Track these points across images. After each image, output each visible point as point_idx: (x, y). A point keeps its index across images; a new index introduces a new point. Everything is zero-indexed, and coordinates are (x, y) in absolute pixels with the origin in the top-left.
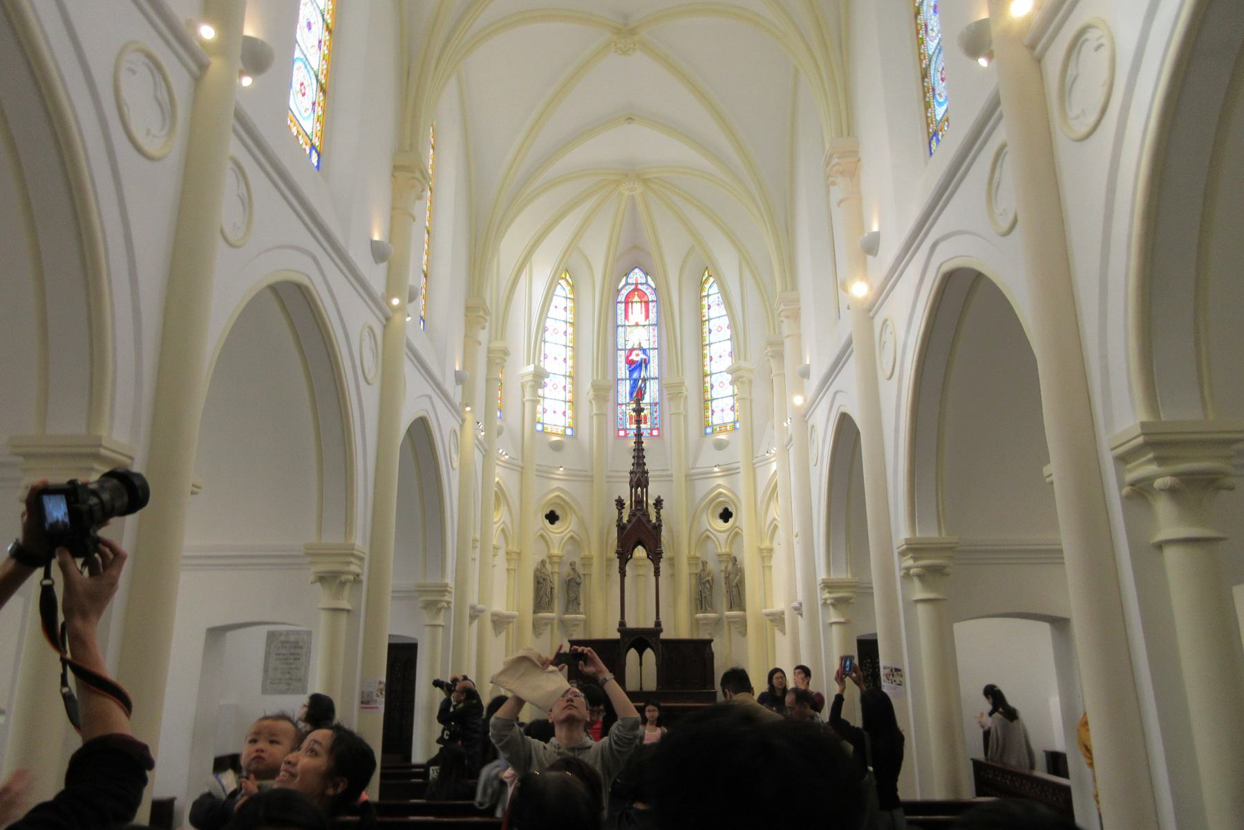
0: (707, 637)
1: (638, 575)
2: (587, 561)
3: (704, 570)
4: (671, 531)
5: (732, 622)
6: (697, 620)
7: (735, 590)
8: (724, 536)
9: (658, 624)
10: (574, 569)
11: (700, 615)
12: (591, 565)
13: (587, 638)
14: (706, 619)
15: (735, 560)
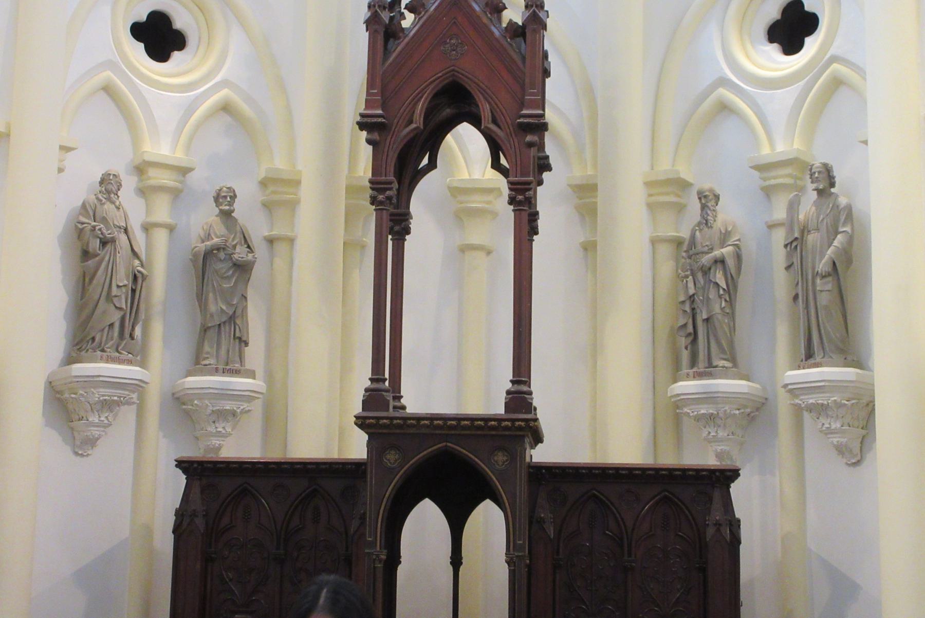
0: (710, 460)
1: (465, 249)
2: (279, 192)
3: (705, 222)
4: (587, 92)
5: (810, 407)
6: (678, 403)
7: (825, 289)
8: (786, 97)
9: (519, 399)
10: (227, 215)
11: (688, 386)
12: (292, 205)
13: (274, 455)
14: (709, 398)
15: (826, 179)
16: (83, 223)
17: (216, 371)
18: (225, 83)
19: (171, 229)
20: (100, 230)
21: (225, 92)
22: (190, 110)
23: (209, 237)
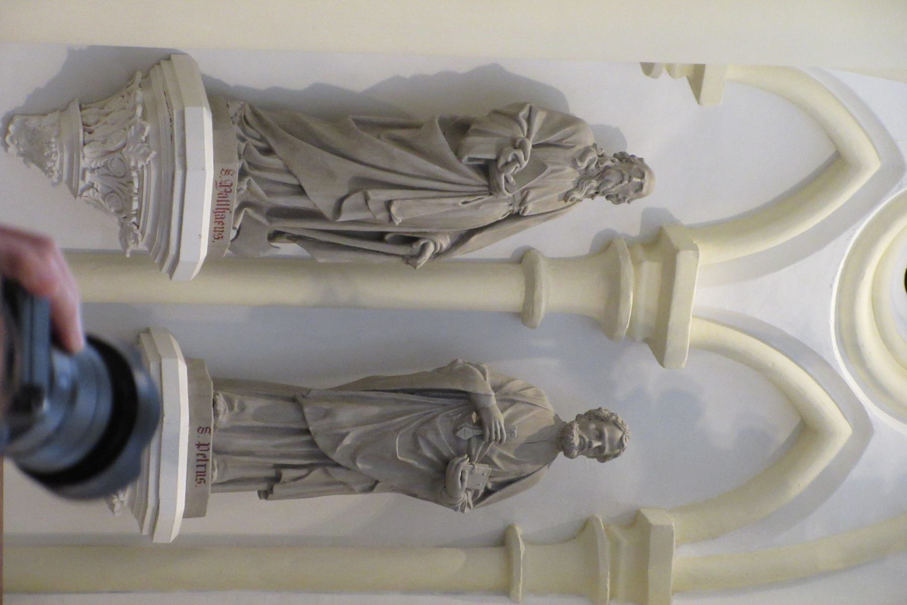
10: (559, 440)
16: (529, 120)
17: (200, 428)
18: (864, 429)
19: (524, 315)
20: (516, 159)
21: (843, 429)
22: (798, 350)
23: (508, 401)
